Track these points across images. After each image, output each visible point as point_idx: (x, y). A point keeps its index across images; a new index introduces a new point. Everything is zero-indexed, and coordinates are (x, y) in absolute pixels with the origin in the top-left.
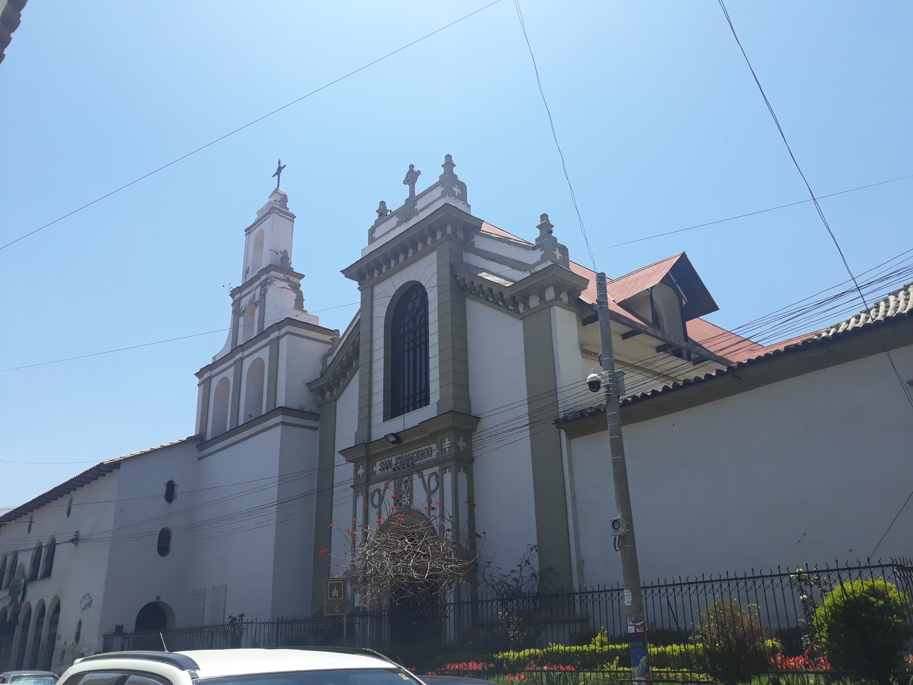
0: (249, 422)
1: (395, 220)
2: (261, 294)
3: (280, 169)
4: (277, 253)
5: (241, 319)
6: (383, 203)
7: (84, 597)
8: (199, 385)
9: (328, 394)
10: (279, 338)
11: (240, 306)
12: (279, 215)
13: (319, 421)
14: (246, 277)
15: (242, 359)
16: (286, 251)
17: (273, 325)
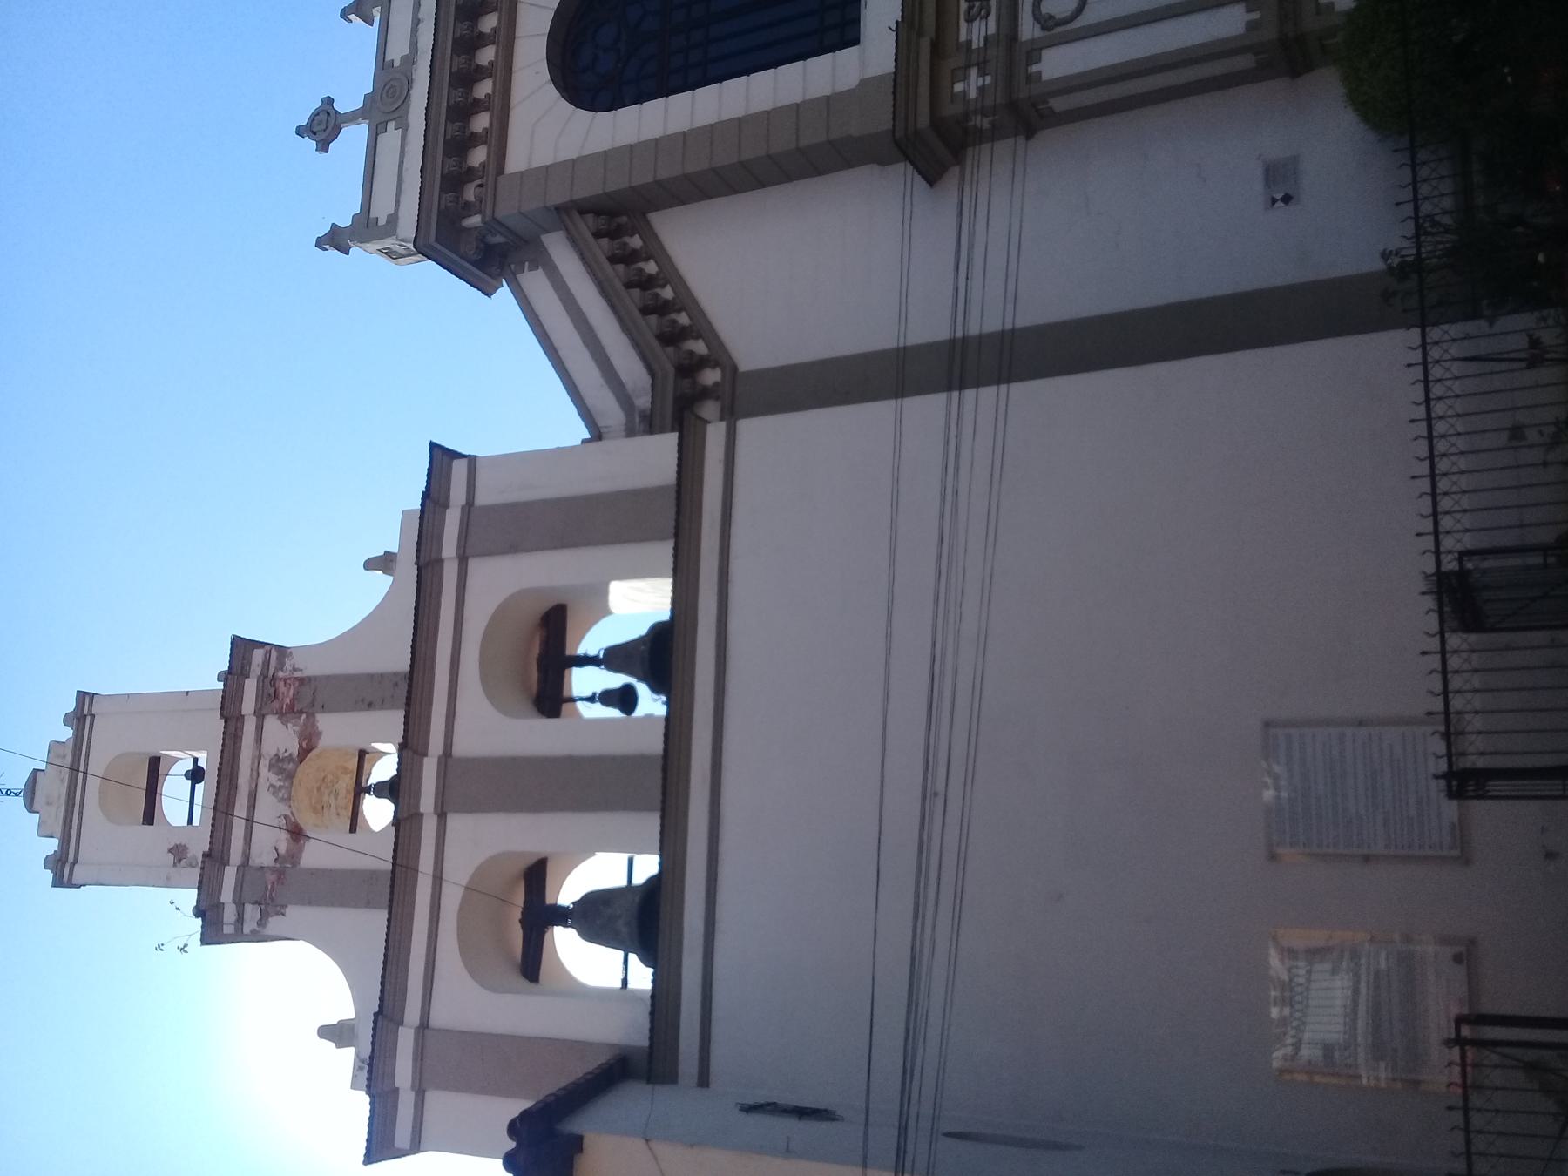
1: (391, 138)
2: (287, 714)
6: (320, 243)
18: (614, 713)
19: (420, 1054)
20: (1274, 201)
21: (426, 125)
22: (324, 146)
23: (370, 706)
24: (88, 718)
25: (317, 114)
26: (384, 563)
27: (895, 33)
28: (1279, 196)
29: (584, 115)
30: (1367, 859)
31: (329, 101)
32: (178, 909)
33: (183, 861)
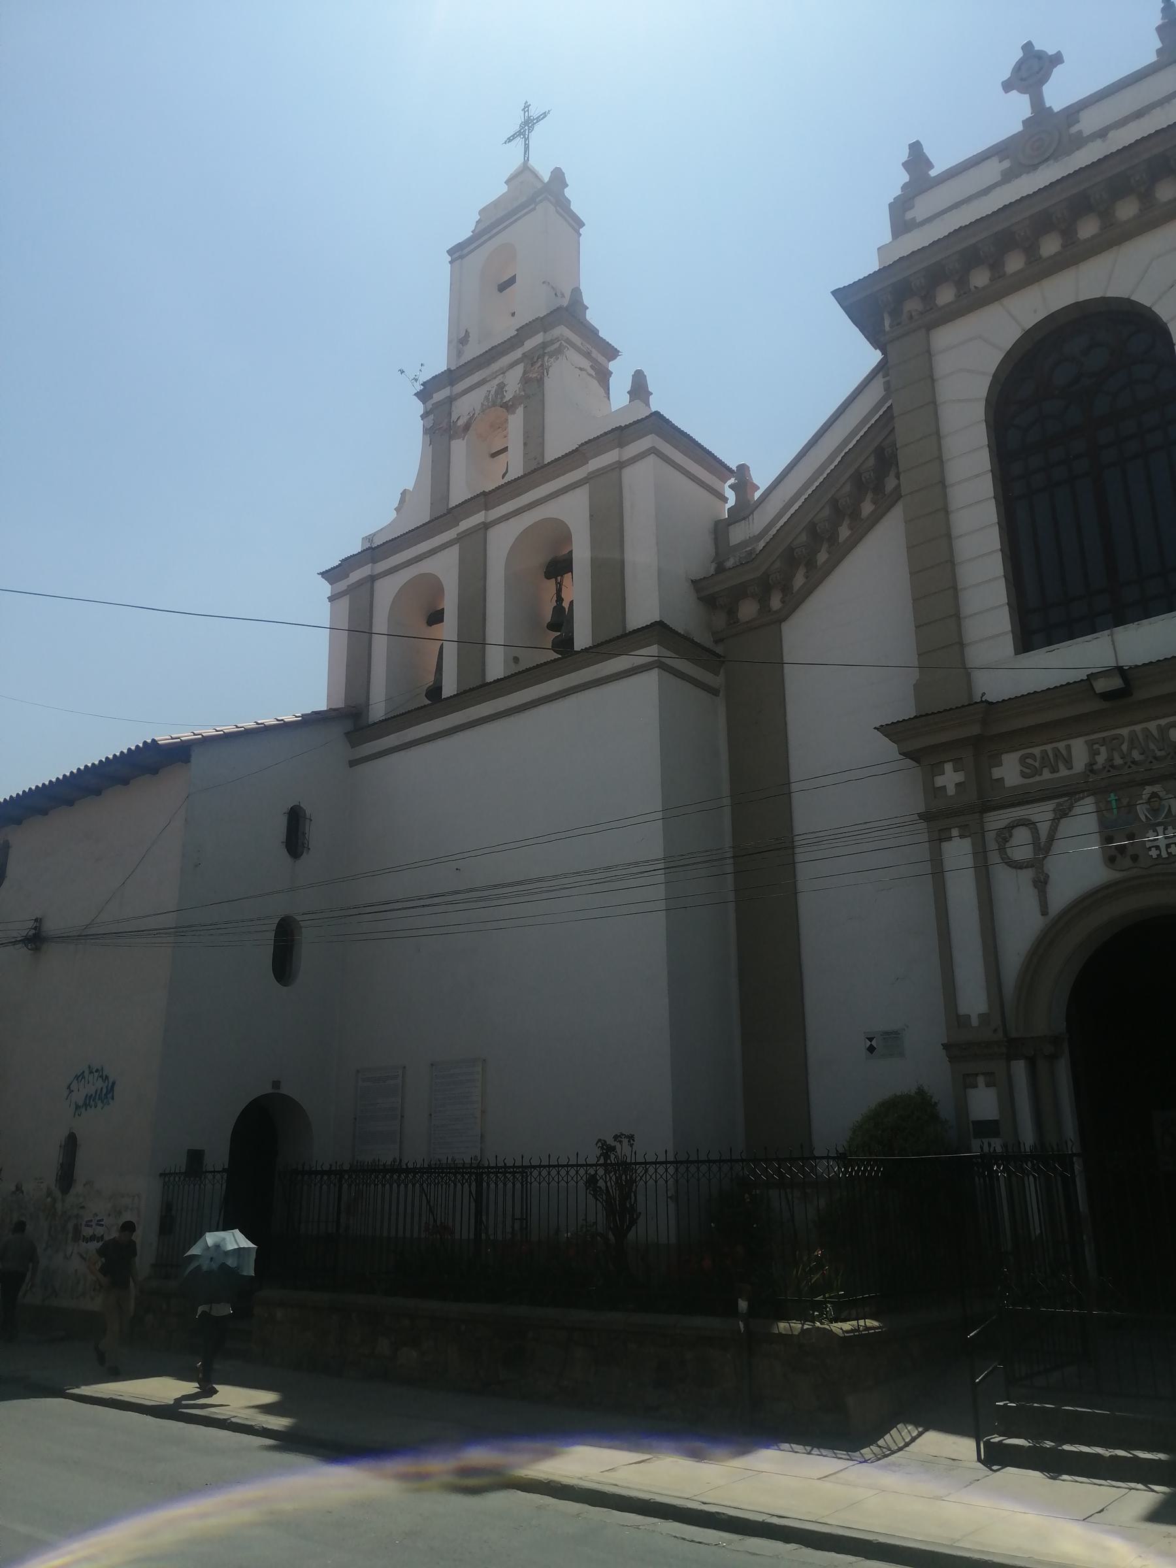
0: (516, 674)
2: (525, 380)
3: (529, 124)
4: (556, 294)
5: (459, 447)
7: (80, 1077)
8: (331, 599)
9: (748, 610)
10: (621, 465)
11: (450, 414)
12: (556, 210)
13: (717, 674)
14: (460, 354)
15: (486, 526)
16: (577, 292)
17: (606, 434)
18: (548, 616)
19: (360, 583)
20: (871, 1039)
21: (966, 226)
22: (1007, 86)
23: (525, 444)
24: (533, 206)
25: (1040, 56)
26: (639, 388)
27: (978, 701)
28: (874, 1043)
29: (980, 387)
30: (431, 1115)
31: (1057, 59)
32: (420, 370)
33: (461, 345)
